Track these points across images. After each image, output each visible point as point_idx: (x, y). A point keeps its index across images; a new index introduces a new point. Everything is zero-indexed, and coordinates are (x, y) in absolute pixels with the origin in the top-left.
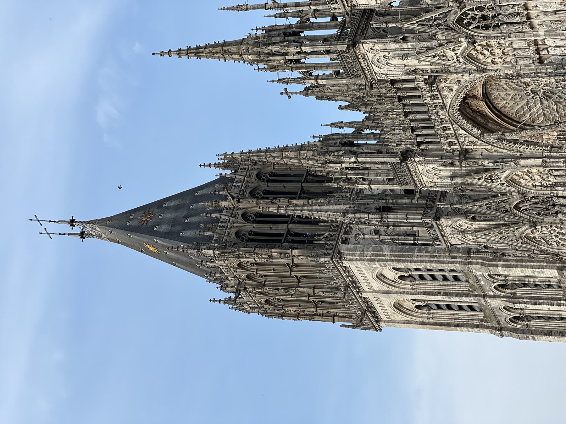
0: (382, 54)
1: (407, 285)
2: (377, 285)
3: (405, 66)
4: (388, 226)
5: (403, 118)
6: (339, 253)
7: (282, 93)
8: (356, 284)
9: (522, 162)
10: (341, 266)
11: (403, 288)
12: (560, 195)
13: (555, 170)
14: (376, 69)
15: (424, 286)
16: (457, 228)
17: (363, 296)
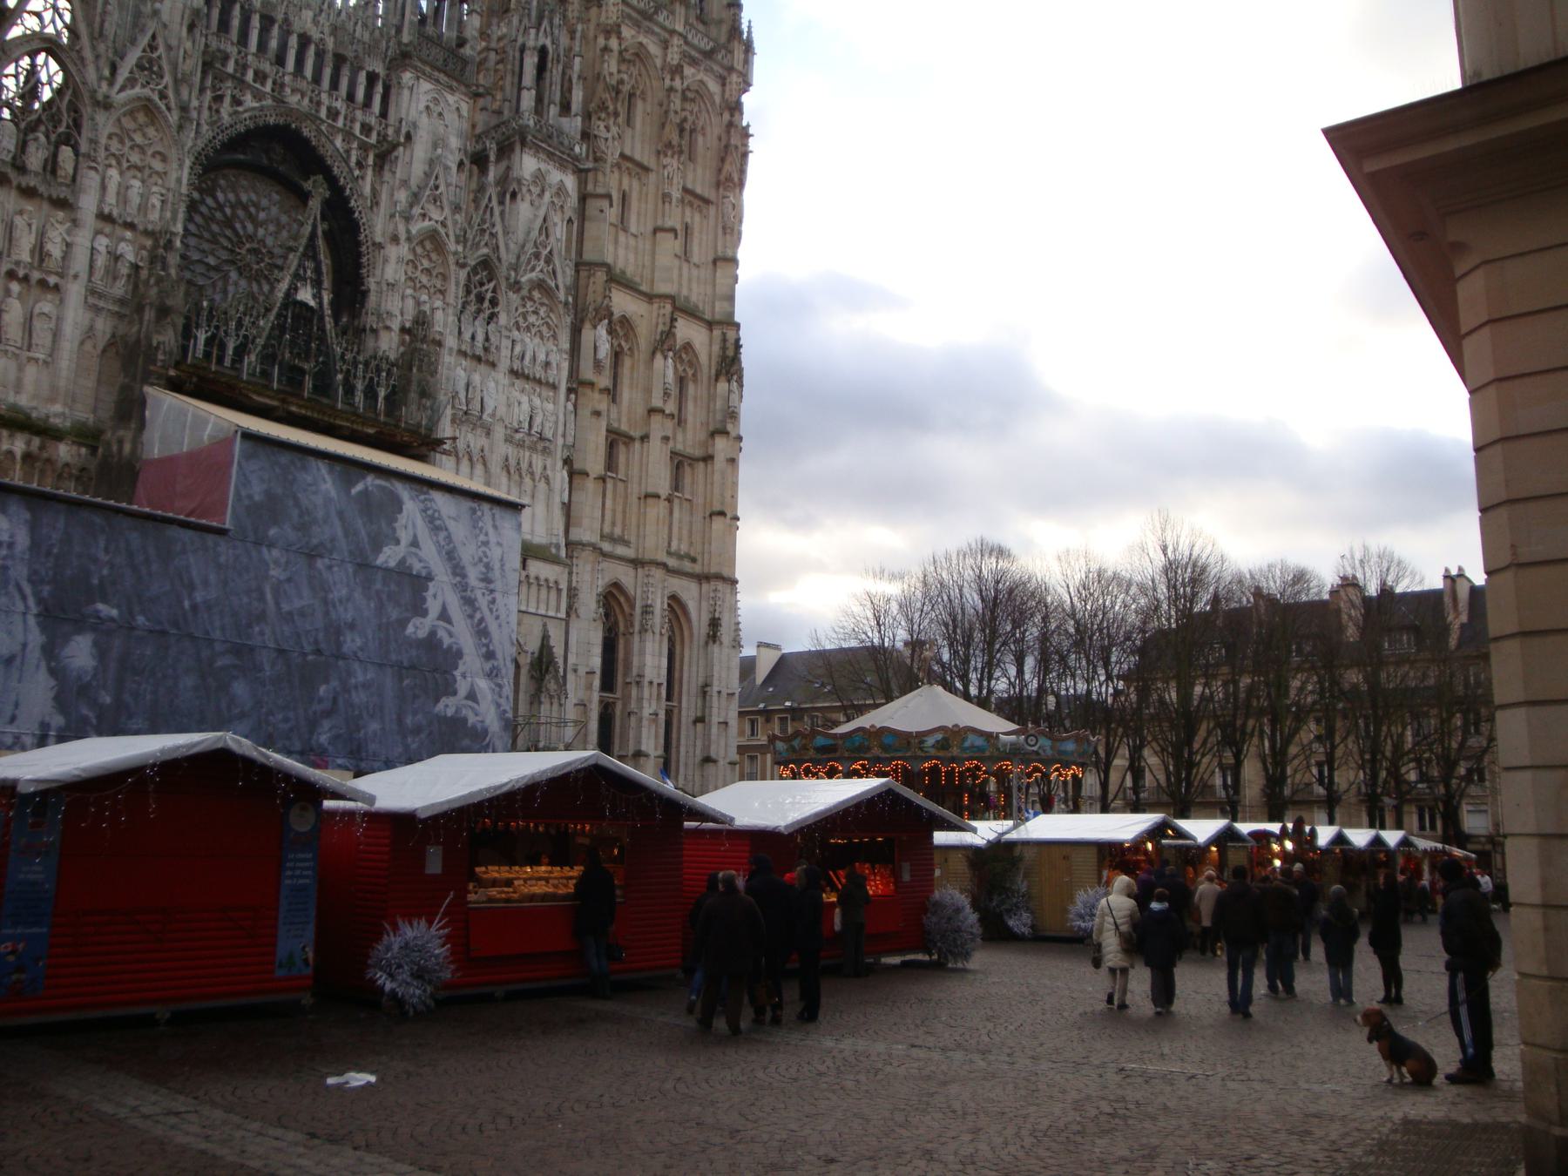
14: (425, 86)
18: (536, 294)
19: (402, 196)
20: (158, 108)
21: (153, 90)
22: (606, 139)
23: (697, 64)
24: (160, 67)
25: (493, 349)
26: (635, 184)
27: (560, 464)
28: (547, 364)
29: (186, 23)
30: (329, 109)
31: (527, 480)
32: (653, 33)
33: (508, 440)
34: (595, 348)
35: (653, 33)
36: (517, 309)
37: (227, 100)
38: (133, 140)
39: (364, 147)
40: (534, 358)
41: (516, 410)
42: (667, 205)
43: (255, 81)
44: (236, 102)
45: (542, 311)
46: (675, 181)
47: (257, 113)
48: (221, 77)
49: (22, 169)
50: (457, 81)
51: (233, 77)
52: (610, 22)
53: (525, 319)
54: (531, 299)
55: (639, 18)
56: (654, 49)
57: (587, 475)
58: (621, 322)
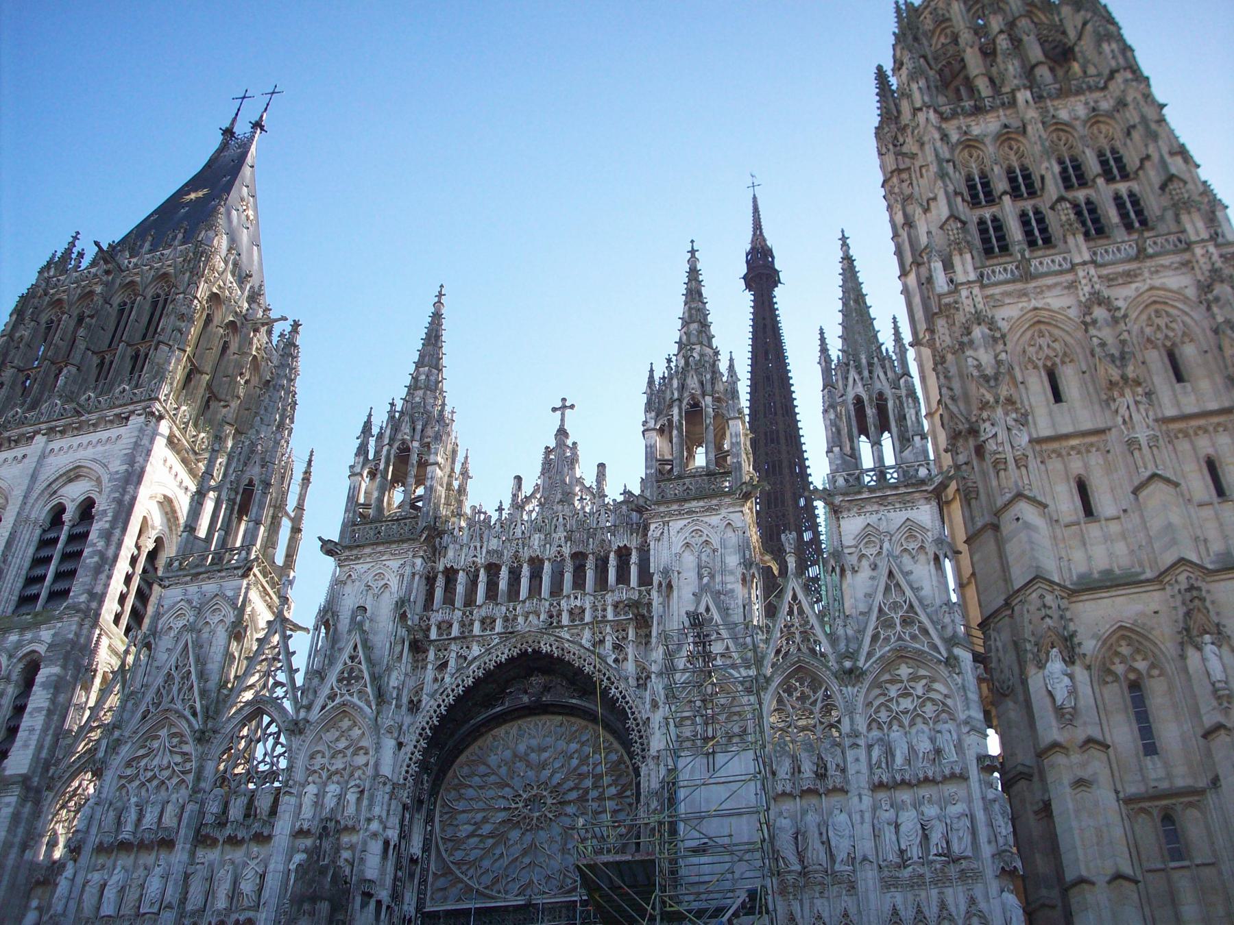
0: (715, 541)
1: (41, 512)
2: (59, 462)
3: (679, 573)
4: (237, 493)
5: (526, 554)
6: (161, 417)
7: (564, 400)
8: (76, 428)
9: (389, 744)
10: (133, 412)
11: (33, 505)
12: (285, 799)
13: (359, 800)
14: (676, 525)
15: (26, 541)
16: (211, 603)
17: (38, 437)
18: (904, 671)
19: (658, 654)
20: (354, 706)
21: (351, 695)
22: (995, 435)
23: (1136, 276)
24: (361, 671)
26: (1095, 459)
27: (994, 886)
30: (571, 612)
32: (1049, 287)
33: (889, 884)
34: (1050, 693)
35: (1049, 287)
36: (870, 704)
37: (452, 663)
39: (620, 627)
41: (889, 834)
42: (1136, 453)
43: (484, 630)
46: (1135, 416)
48: (442, 647)
49: (221, 822)
51: (455, 639)
52: (968, 316)
53: (889, 710)
55: (1019, 286)
56: (1057, 300)
57: (1093, 884)
58: (1123, 637)
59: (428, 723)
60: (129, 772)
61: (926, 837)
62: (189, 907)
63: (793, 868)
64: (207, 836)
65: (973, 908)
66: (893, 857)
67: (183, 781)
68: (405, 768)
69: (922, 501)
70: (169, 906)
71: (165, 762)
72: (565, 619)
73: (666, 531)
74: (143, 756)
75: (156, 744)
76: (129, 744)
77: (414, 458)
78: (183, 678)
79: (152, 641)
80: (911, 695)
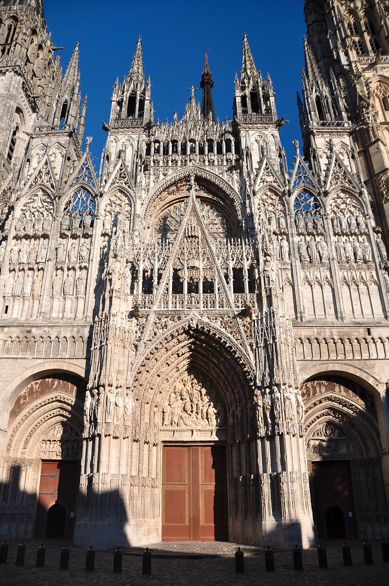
14: (251, 132)
18: (342, 195)
22: (369, 118)
24: (125, 174)
25: (319, 227)
28: (358, 224)
29: (136, 156)
30: (209, 161)
31: (362, 287)
36: (331, 205)
38: (115, 203)
40: (349, 225)
41: (342, 251)
44: (165, 175)
45: (348, 201)
47: (175, 175)
50: (267, 124)
51: (161, 167)
53: (339, 208)
54: (339, 197)
59: (152, 197)
60: (24, 208)
61: (354, 253)
62: (58, 260)
63: (307, 260)
64: (64, 234)
65: (372, 279)
66: (344, 259)
67: (51, 213)
68: (144, 213)
69: (346, 136)
70: (49, 260)
71: (41, 205)
72: (207, 163)
73: (247, 134)
74: (31, 202)
75: (35, 198)
76: (25, 197)
77: (138, 98)
78: (46, 173)
79: (30, 159)
80: (346, 203)
